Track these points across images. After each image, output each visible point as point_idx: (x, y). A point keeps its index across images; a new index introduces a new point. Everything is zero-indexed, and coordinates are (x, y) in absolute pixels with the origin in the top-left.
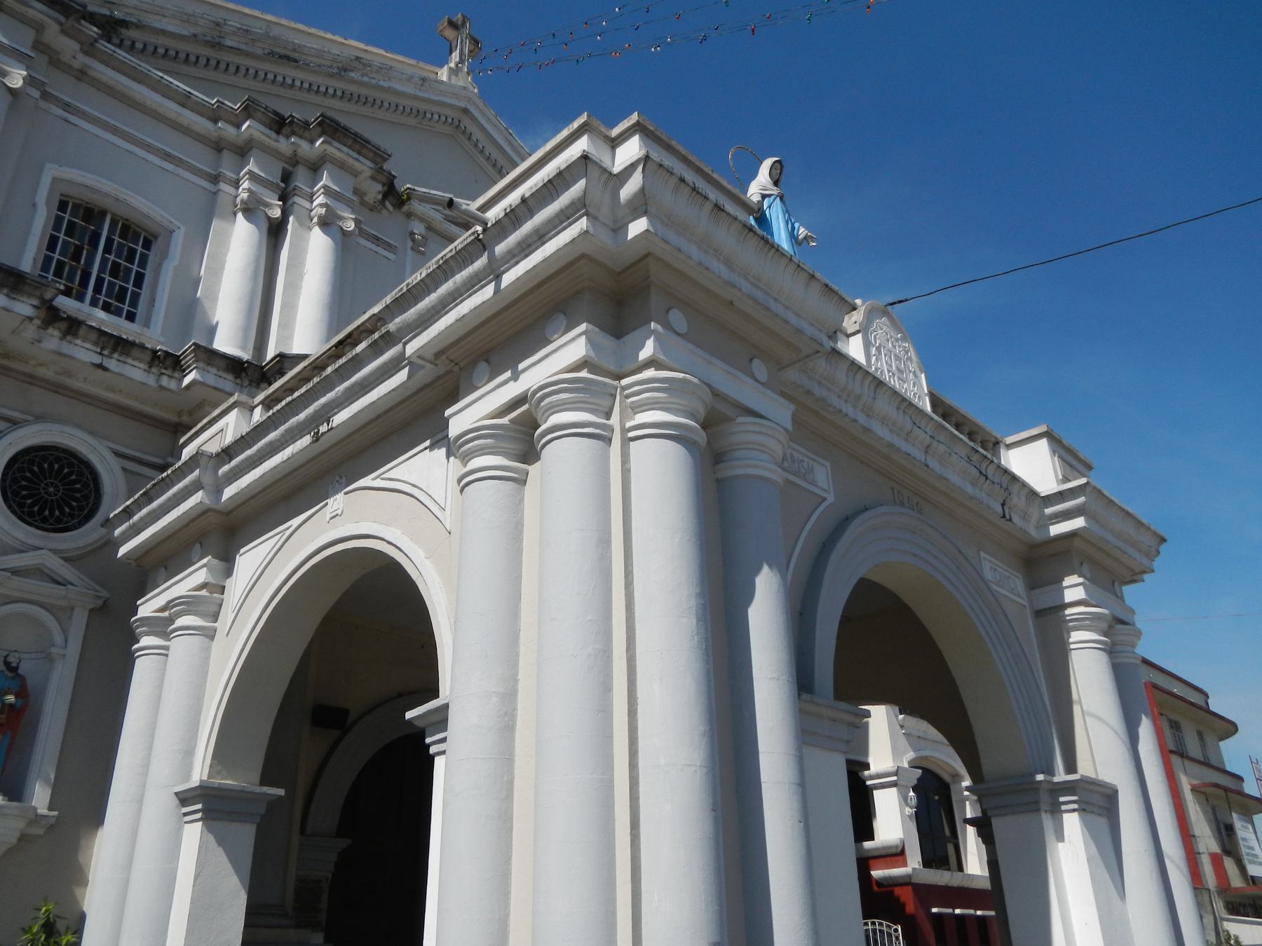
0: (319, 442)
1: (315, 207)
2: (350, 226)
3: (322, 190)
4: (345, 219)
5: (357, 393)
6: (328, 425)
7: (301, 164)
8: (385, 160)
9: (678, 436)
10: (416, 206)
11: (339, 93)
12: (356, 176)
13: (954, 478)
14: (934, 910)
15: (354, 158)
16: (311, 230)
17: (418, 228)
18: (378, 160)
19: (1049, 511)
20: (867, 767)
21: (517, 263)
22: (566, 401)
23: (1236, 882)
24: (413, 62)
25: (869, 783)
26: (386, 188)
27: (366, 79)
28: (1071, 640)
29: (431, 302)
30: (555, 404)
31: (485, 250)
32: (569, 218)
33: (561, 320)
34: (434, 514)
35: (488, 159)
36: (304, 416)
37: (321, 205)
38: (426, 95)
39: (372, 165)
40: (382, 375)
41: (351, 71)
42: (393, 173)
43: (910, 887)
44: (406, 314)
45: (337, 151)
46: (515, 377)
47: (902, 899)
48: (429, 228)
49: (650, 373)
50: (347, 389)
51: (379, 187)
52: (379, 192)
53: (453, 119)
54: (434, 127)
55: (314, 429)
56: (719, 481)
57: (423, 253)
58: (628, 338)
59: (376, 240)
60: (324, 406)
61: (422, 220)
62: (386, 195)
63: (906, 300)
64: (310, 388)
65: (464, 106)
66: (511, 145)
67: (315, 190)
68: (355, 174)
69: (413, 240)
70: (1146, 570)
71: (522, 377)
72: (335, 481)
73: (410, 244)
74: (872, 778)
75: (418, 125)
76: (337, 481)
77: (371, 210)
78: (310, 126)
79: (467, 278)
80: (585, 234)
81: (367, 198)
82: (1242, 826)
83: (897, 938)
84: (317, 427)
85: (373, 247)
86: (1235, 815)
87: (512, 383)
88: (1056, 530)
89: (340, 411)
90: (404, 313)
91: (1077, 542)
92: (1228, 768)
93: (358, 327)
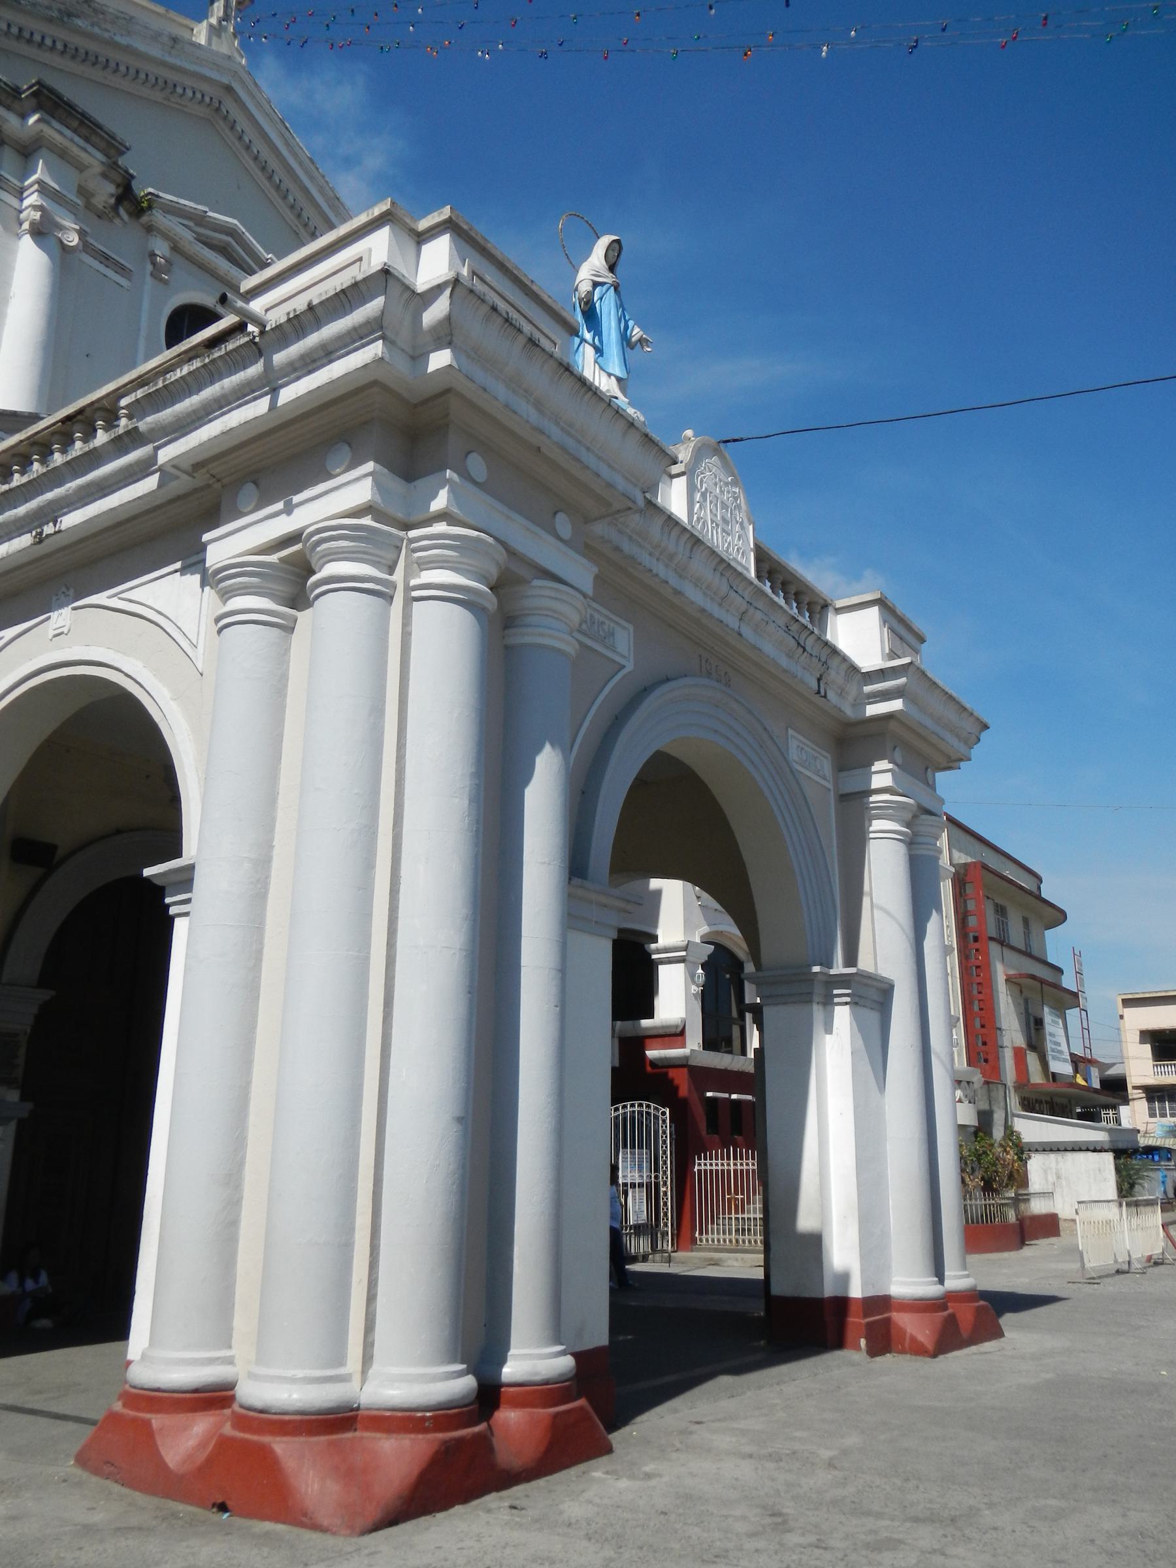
0: (42, 545)
1: (27, 208)
2: (73, 239)
3: (36, 187)
4: (68, 229)
5: (93, 494)
6: (55, 526)
7: (8, 145)
8: (121, 153)
9: (468, 601)
10: (158, 217)
11: (59, 46)
12: (81, 171)
13: (768, 648)
14: (709, 1094)
15: (78, 146)
16: (20, 238)
17: (161, 248)
18: (113, 152)
19: (868, 689)
20: (655, 939)
21: (298, 378)
22: (345, 550)
23: (1036, 1077)
24: (160, 9)
25: (654, 957)
26: (120, 190)
27: (96, 30)
28: (871, 829)
29: (191, 405)
30: (333, 551)
31: (261, 356)
32: (362, 338)
33: (345, 452)
34: (183, 650)
35: (256, 158)
36: (24, 511)
37: (36, 208)
38: (178, 62)
39: (104, 159)
40: (126, 478)
41: (78, 17)
42: (131, 171)
43: (686, 1070)
44: (160, 414)
45: (57, 133)
46: (289, 510)
47: (676, 1082)
48: (175, 248)
49: (441, 528)
50: (81, 488)
51: (111, 189)
52: (112, 195)
53: (211, 99)
54: (186, 106)
55: (36, 528)
56: (507, 647)
57: (166, 282)
58: (420, 483)
59: (105, 259)
60: (50, 503)
61: (166, 236)
62: (120, 200)
63: (742, 440)
64: (34, 479)
65: (227, 82)
66: (287, 144)
67: (26, 183)
68: (81, 167)
69: (154, 264)
70: (963, 757)
71: (296, 511)
72: (60, 593)
73: (149, 267)
74: (658, 951)
75: (165, 102)
76: (63, 593)
77: (99, 217)
78: (20, 94)
79: (238, 385)
80: (379, 361)
81: (95, 201)
82: (1053, 1021)
83: (664, 1121)
84: (41, 526)
85: (102, 268)
86: (1046, 1009)
87: (284, 516)
88: (874, 710)
89: (70, 512)
90: (158, 411)
91: (893, 725)
93: (92, 403)
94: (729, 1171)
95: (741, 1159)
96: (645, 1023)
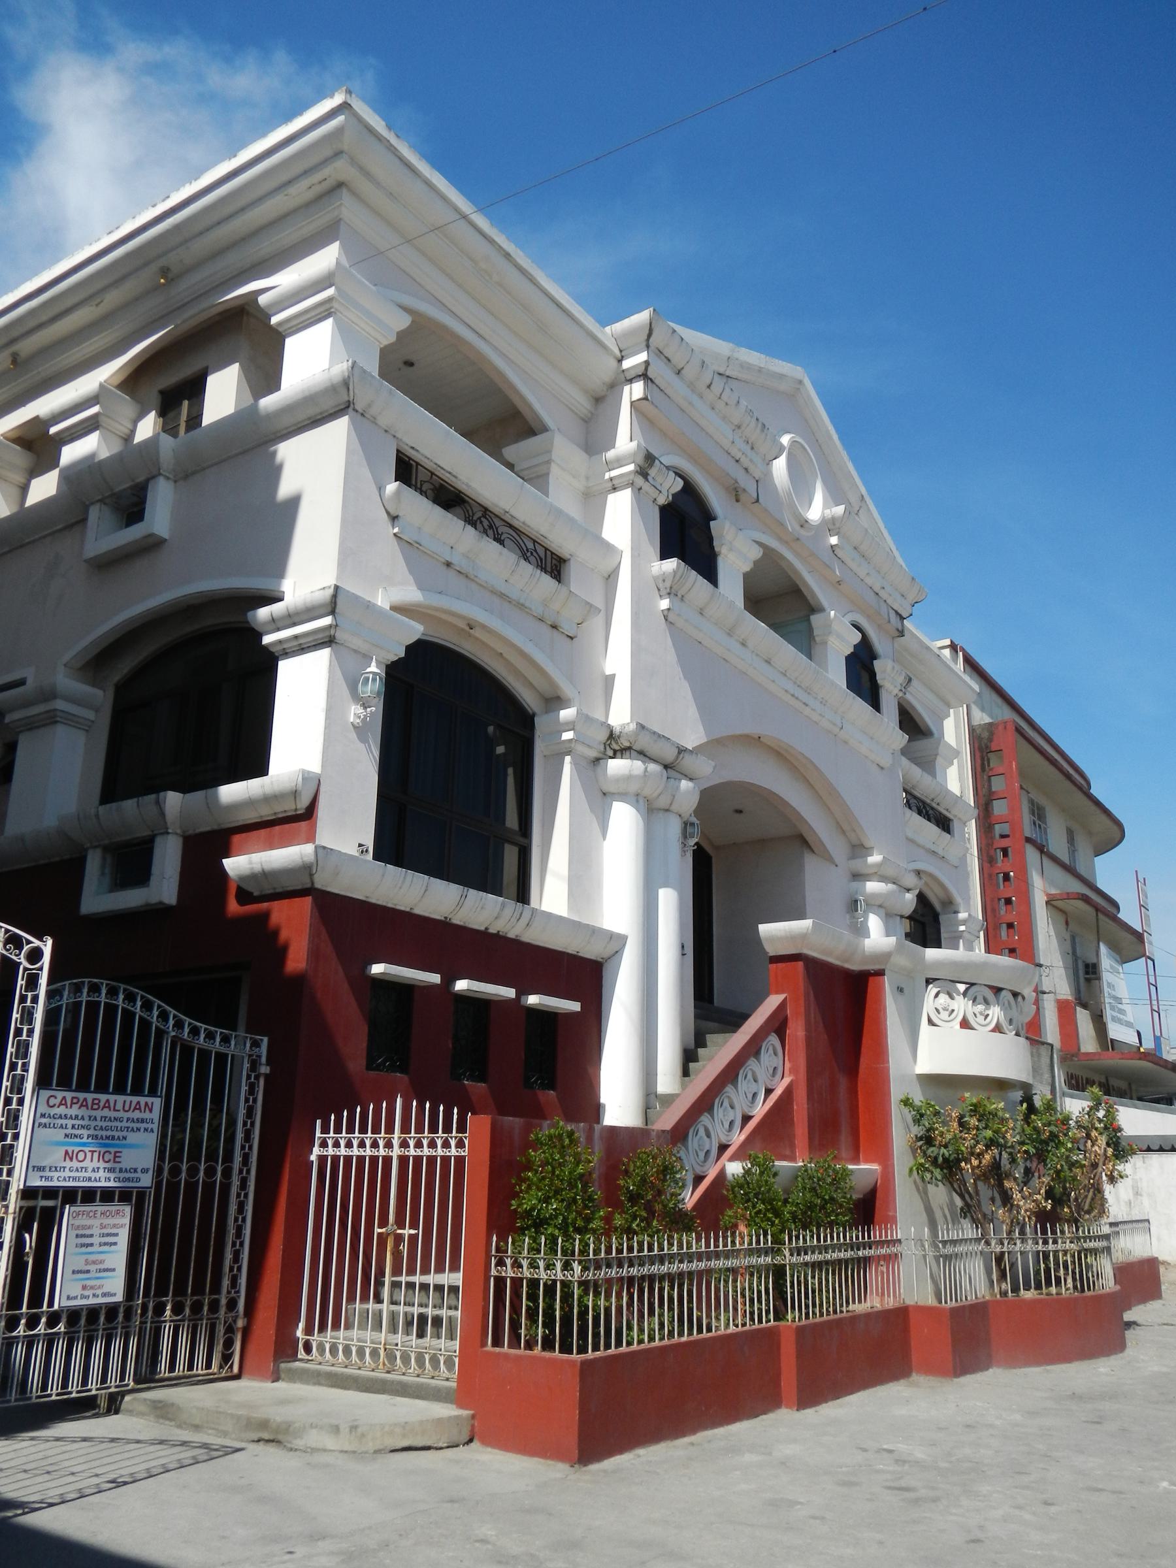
14: (377, 969)
23: (1088, 1043)
25: (267, 639)
47: (284, 935)
74: (276, 624)
82: (1112, 967)
83: (32, 982)
86: (1103, 949)
92: (1099, 885)
94: (388, 1160)
95: (419, 1130)
96: (230, 792)
